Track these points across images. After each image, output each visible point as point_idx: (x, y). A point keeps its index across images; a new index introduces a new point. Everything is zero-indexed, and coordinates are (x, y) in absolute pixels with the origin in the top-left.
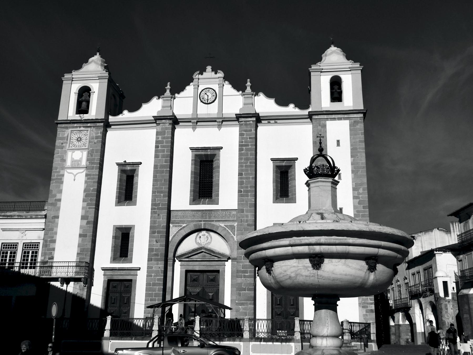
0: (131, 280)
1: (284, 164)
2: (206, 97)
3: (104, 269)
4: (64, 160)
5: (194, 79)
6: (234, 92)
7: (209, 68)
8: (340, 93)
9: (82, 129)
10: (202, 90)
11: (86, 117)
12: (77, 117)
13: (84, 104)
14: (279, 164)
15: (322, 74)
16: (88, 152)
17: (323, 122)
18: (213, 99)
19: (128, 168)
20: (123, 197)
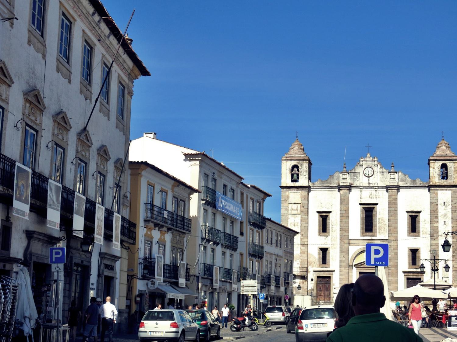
0: (329, 278)
1: (414, 214)
2: (367, 173)
3: (314, 271)
4: (287, 210)
5: (361, 162)
6: (384, 170)
7: (368, 155)
8: (447, 173)
9: (296, 191)
10: (365, 169)
11: (297, 184)
12: (293, 184)
13: (295, 176)
14: (411, 214)
15: (436, 162)
16: (301, 205)
17: (436, 191)
18: (372, 174)
19: (324, 214)
20: (321, 231)
